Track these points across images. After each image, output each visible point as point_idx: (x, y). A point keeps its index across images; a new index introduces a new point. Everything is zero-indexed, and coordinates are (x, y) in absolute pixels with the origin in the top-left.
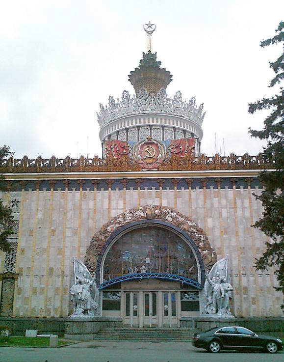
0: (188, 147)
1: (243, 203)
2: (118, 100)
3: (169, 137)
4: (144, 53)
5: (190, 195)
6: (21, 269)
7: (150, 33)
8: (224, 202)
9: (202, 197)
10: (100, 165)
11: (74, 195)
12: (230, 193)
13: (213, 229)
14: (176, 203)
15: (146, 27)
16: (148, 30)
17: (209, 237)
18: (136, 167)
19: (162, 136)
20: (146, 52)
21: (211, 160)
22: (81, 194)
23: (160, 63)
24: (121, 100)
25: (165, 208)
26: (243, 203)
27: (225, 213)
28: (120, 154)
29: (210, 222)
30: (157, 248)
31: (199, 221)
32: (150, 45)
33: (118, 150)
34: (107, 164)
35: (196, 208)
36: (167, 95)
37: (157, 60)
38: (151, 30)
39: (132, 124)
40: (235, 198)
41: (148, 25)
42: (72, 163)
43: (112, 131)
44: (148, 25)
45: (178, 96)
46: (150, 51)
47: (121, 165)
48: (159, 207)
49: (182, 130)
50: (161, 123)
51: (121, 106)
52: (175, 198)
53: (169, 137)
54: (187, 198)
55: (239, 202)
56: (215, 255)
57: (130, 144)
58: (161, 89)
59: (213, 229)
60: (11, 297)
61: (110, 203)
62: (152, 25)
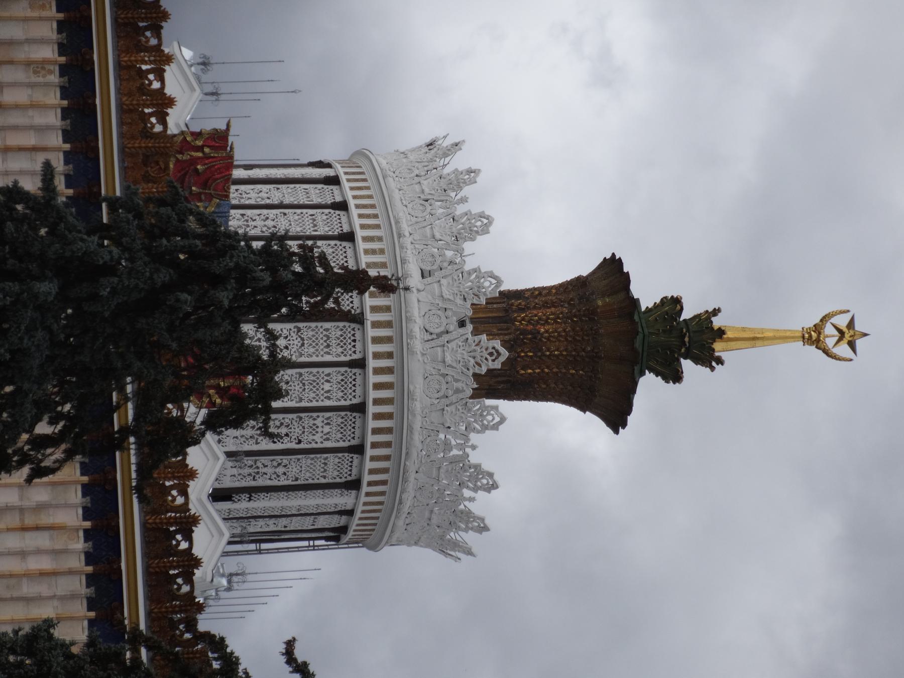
1: (39, 552)
2: (464, 200)
3: (327, 386)
4: (716, 312)
10: (145, 118)
11: (42, 41)
15: (842, 321)
16: (829, 330)
19: (328, 358)
20: (717, 322)
22: (45, 62)
23: (674, 376)
24: (460, 209)
26: (39, 552)
28: (185, 175)
32: (754, 339)
33: (197, 170)
34: (147, 134)
38: (830, 342)
39: (366, 252)
41: (851, 324)
42: (146, 28)
43: (352, 189)
44: (851, 324)
46: (721, 333)
47: (147, 179)
49: (363, 437)
50: (377, 356)
51: (441, 211)
53: (327, 386)
55: (42, 540)
57: (218, 206)
58: (502, 350)
61: (21, 149)
62: (852, 345)
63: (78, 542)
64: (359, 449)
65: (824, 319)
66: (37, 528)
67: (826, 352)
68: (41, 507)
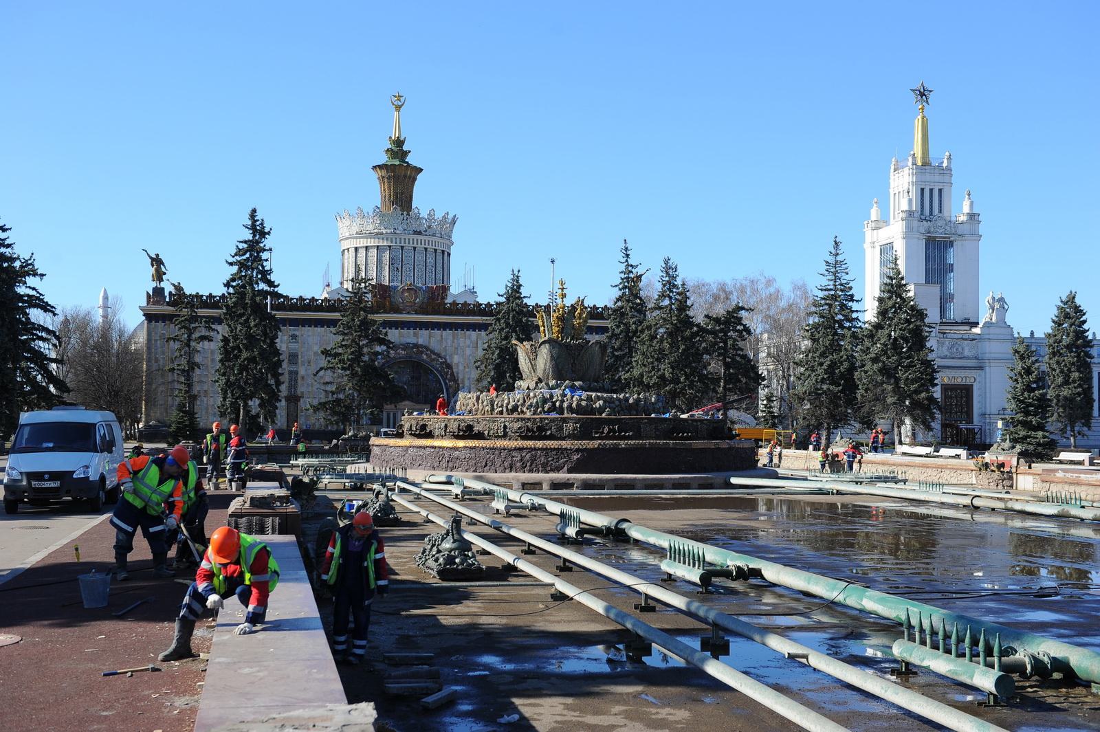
0: (442, 293)
5: (442, 336)
6: (302, 393)
7: (398, 108)
8: (468, 342)
9: (451, 337)
12: (473, 334)
13: (457, 365)
14: (430, 342)
17: (454, 370)
18: (397, 311)
21: (460, 305)
25: (422, 346)
27: (468, 351)
29: (456, 359)
30: (412, 378)
31: (448, 357)
35: (446, 346)
36: (420, 214)
37: (405, 148)
38: (400, 104)
40: (477, 340)
41: (395, 97)
44: (395, 97)
45: (431, 214)
48: (416, 346)
50: (413, 243)
52: (430, 338)
54: (439, 338)
56: (459, 384)
59: (457, 365)
60: (295, 414)
63: (481, 334)
64: (436, 250)
65: (393, 104)
66: (477, 343)
67: (402, 105)
68: (471, 342)
